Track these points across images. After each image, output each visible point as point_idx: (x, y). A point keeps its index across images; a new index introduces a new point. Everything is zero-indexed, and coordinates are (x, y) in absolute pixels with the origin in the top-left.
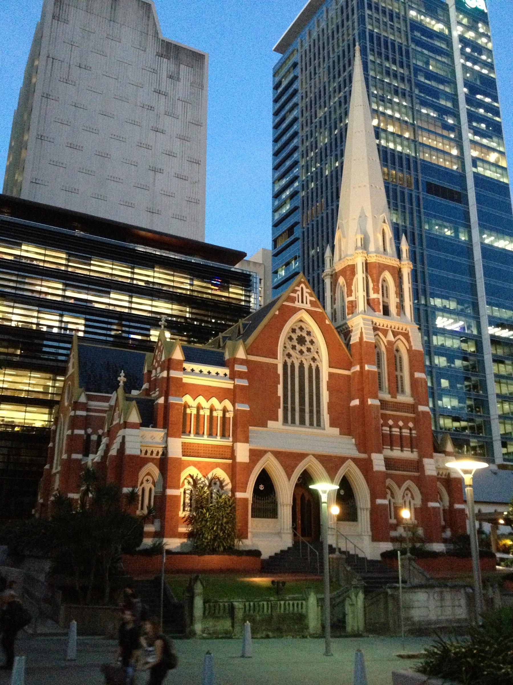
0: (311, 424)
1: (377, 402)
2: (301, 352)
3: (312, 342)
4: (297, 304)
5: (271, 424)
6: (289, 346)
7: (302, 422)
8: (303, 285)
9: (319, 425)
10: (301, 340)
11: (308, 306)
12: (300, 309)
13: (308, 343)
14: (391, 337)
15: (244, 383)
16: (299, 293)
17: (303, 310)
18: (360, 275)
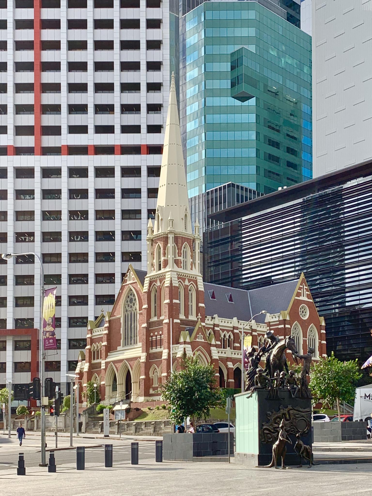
0: (134, 343)
1: (145, 325)
2: (131, 307)
3: (135, 300)
4: (128, 283)
5: (119, 348)
6: (127, 306)
7: (131, 344)
8: (130, 271)
9: (137, 343)
10: (131, 301)
11: (132, 282)
12: (128, 284)
13: (134, 301)
14: (158, 284)
15: (106, 332)
16: (129, 276)
17: (130, 285)
18: (171, 244)
